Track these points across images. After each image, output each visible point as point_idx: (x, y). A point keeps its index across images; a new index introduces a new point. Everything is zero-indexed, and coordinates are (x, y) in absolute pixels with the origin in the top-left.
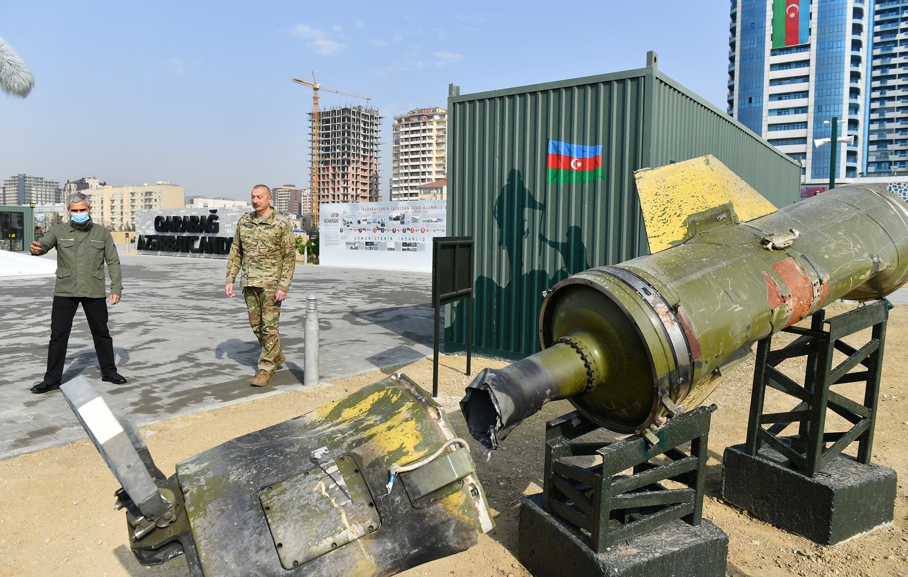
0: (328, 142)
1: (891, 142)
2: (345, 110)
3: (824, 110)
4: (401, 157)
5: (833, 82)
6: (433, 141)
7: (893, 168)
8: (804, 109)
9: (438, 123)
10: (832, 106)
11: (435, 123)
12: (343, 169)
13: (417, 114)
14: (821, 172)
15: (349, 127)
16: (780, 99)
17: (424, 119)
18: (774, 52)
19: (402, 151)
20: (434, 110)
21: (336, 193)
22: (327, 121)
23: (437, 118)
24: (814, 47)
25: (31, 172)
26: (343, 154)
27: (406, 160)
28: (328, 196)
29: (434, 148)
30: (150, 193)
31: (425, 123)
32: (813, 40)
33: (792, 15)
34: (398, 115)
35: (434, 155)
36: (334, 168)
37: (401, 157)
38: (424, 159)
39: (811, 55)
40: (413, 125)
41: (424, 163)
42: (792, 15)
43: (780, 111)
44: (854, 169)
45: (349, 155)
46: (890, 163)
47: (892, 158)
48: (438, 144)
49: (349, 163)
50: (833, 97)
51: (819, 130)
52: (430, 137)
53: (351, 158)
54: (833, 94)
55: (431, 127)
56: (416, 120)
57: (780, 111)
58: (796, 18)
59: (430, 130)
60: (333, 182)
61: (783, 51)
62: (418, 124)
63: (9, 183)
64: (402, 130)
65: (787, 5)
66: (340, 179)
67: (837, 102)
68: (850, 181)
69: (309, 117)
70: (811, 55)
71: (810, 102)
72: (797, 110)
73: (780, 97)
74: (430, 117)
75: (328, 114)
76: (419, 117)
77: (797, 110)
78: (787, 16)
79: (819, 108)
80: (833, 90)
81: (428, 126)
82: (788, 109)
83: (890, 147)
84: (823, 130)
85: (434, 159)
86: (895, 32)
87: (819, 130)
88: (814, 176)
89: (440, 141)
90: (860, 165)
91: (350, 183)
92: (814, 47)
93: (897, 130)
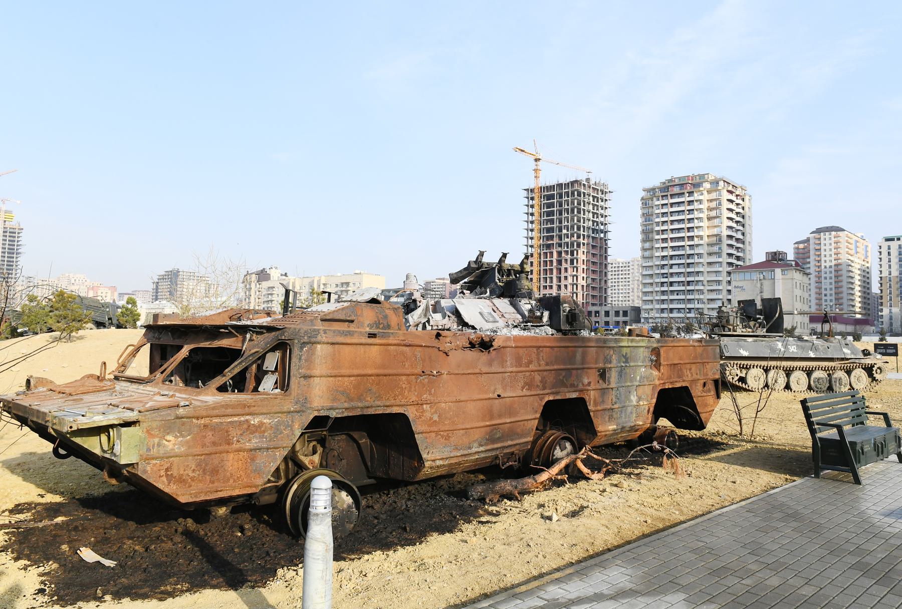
0: (552, 221)
2: (573, 183)
4: (657, 237)
6: (704, 215)
9: (709, 192)
11: (705, 193)
12: (572, 254)
13: (677, 182)
15: (579, 204)
17: (689, 188)
19: (657, 228)
20: (702, 176)
21: (563, 283)
22: (551, 197)
23: (707, 185)
25: (184, 265)
26: (572, 236)
27: (664, 240)
28: (551, 287)
29: (705, 223)
30: (347, 284)
31: (691, 193)
34: (650, 185)
35: (705, 233)
36: (560, 253)
37: (657, 237)
38: (691, 238)
40: (672, 196)
41: (691, 243)
45: (579, 237)
48: (709, 219)
49: (579, 245)
52: (700, 210)
53: (581, 240)
55: (701, 198)
56: (676, 190)
59: (700, 201)
60: (559, 271)
62: (681, 194)
63: (162, 278)
64: (657, 203)
66: (568, 266)
69: (525, 193)
74: (697, 185)
75: (551, 188)
76: (682, 185)
81: (696, 196)
85: (706, 239)
89: (713, 213)
91: (580, 270)
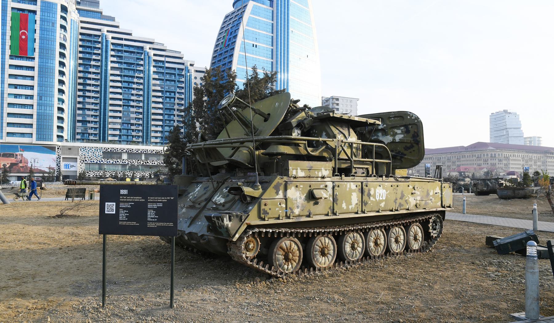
1: (89, 122)
3: (43, 99)
5: (48, 83)
7: (91, 137)
8: (31, 97)
10: (48, 98)
14: (42, 137)
16: (16, 88)
18: (12, 57)
24: (37, 59)
32: (36, 55)
33: (24, 37)
39: (35, 63)
42: (24, 37)
43: (16, 96)
44: (62, 137)
46: (89, 134)
47: (90, 131)
50: (48, 93)
51: (40, 111)
54: (48, 90)
57: (16, 96)
58: (26, 40)
61: (17, 57)
65: (21, 30)
67: (51, 96)
68: (60, 144)
70: (35, 63)
71: (35, 92)
72: (27, 97)
73: (16, 86)
77: (27, 97)
78: (21, 37)
79: (40, 97)
80: (48, 88)
82: (21, 95)
83: (89, 125)
84: (43, 111)
86: (90, 60)
87: (40, 111)
88: (38, 139)
90: (66, 134)
92: (37, 59)
93: (92, 116)
